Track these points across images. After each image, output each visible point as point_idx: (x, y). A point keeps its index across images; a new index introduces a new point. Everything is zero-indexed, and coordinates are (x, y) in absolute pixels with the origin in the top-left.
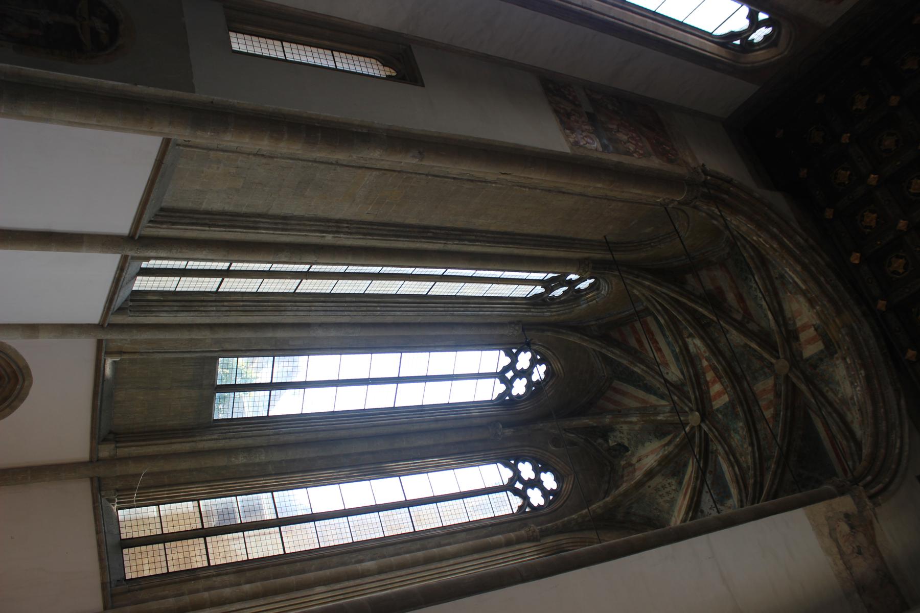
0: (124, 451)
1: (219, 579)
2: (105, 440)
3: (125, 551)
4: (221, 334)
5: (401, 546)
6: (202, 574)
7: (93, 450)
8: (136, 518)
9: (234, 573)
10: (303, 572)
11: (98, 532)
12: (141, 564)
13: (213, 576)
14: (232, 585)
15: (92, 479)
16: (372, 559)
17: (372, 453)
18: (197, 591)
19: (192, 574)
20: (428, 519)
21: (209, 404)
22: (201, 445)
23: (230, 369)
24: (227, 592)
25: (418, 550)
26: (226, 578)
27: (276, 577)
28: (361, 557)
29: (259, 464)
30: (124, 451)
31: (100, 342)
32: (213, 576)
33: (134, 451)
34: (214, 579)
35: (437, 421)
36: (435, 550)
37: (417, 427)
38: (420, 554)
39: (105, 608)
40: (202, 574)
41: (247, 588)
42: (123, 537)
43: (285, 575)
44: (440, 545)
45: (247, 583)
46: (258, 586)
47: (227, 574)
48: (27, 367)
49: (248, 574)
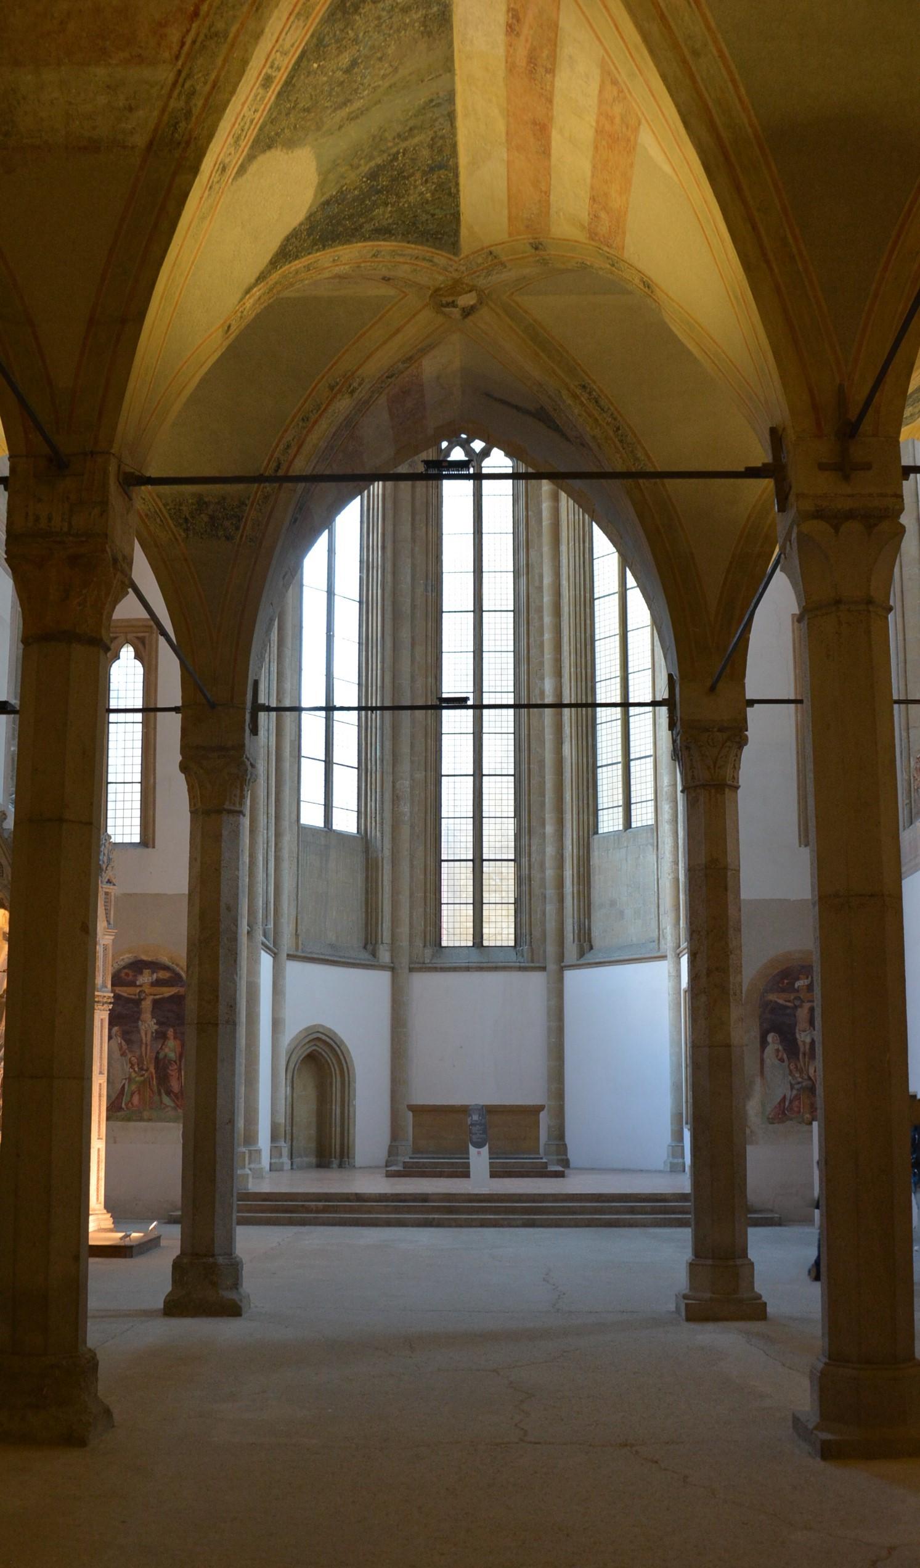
0: (387, 937)
1: (534, 856)
2: (374, 954)
3: (485, 943)
4: (285, 824)
5: (531, 640)
6: (525, 871)
7: (382, 967)
8: (456, 929)
9: (530, 839)
10: (542, 764)
11: (468, 969)
12: (500, 929)
13: (529, 861)
14: (543, 844)
15: (411, 970)
16: (542, 679)
17: (413, 645)
18: (543, 880)
19: (521, 880)
20: (500, 590)
21: (342, 836)
22: (387, 853)
23: (311, 816)
24: (550, 850)
25: (541, 618)
26: (533, 848)
27: (543, 795)
28: (537, 692)
29: (412, 788)
30: (387, 938)
31: (290, 957)
32: (529, 861)
33: (387, 924)
34: (533, 860)
35: (384, 548)
36: (545, 600)
37: (389, 578)
38: (547, 620)
39: (544, 969)
40: (525, 871)
41: (549, 829)
42: (470, 944)
43: (542, 784)
44: (540, 589)
45: (543, 825)
46: (549, 816)
47: (530, 846)
48: (306, 1029)
49: (534, 823)
